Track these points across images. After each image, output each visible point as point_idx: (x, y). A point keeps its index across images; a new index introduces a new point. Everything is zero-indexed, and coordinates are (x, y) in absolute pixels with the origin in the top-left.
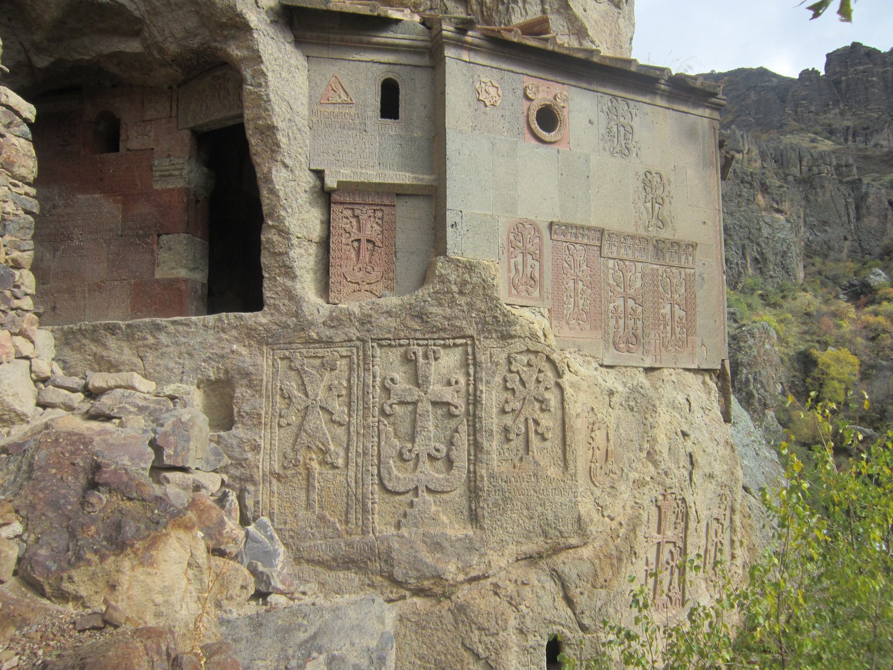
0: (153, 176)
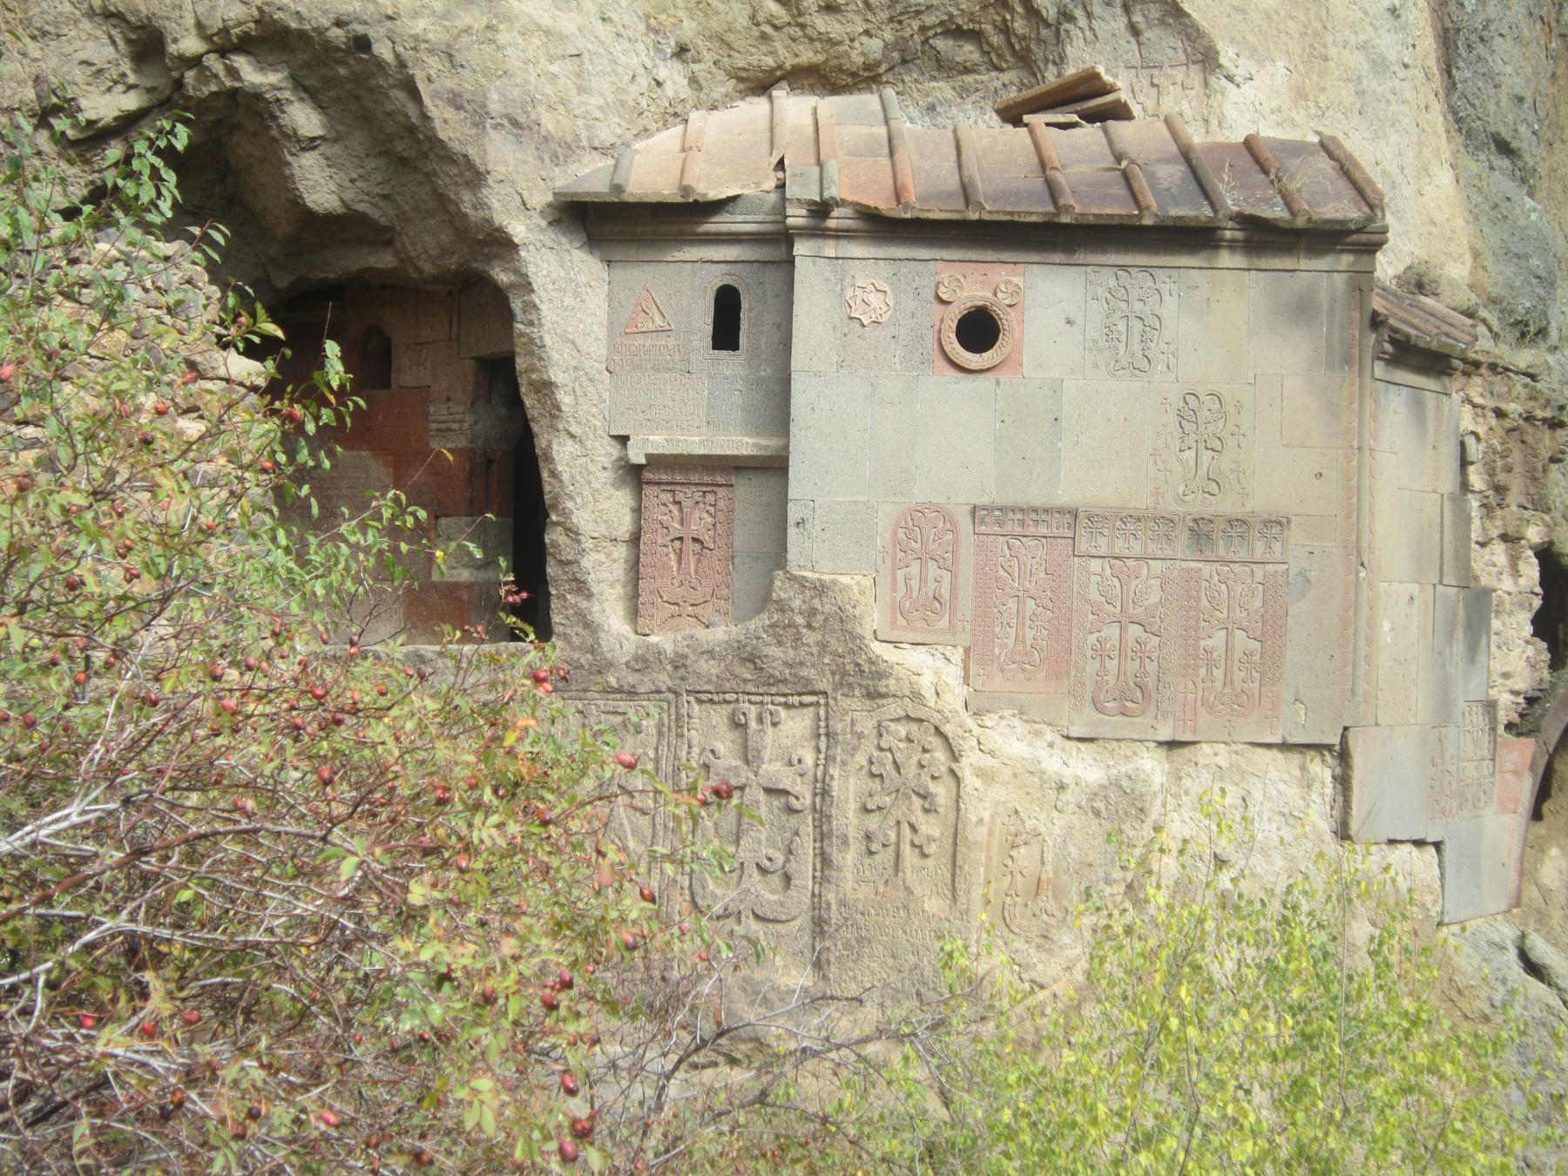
0: (429, 430)
